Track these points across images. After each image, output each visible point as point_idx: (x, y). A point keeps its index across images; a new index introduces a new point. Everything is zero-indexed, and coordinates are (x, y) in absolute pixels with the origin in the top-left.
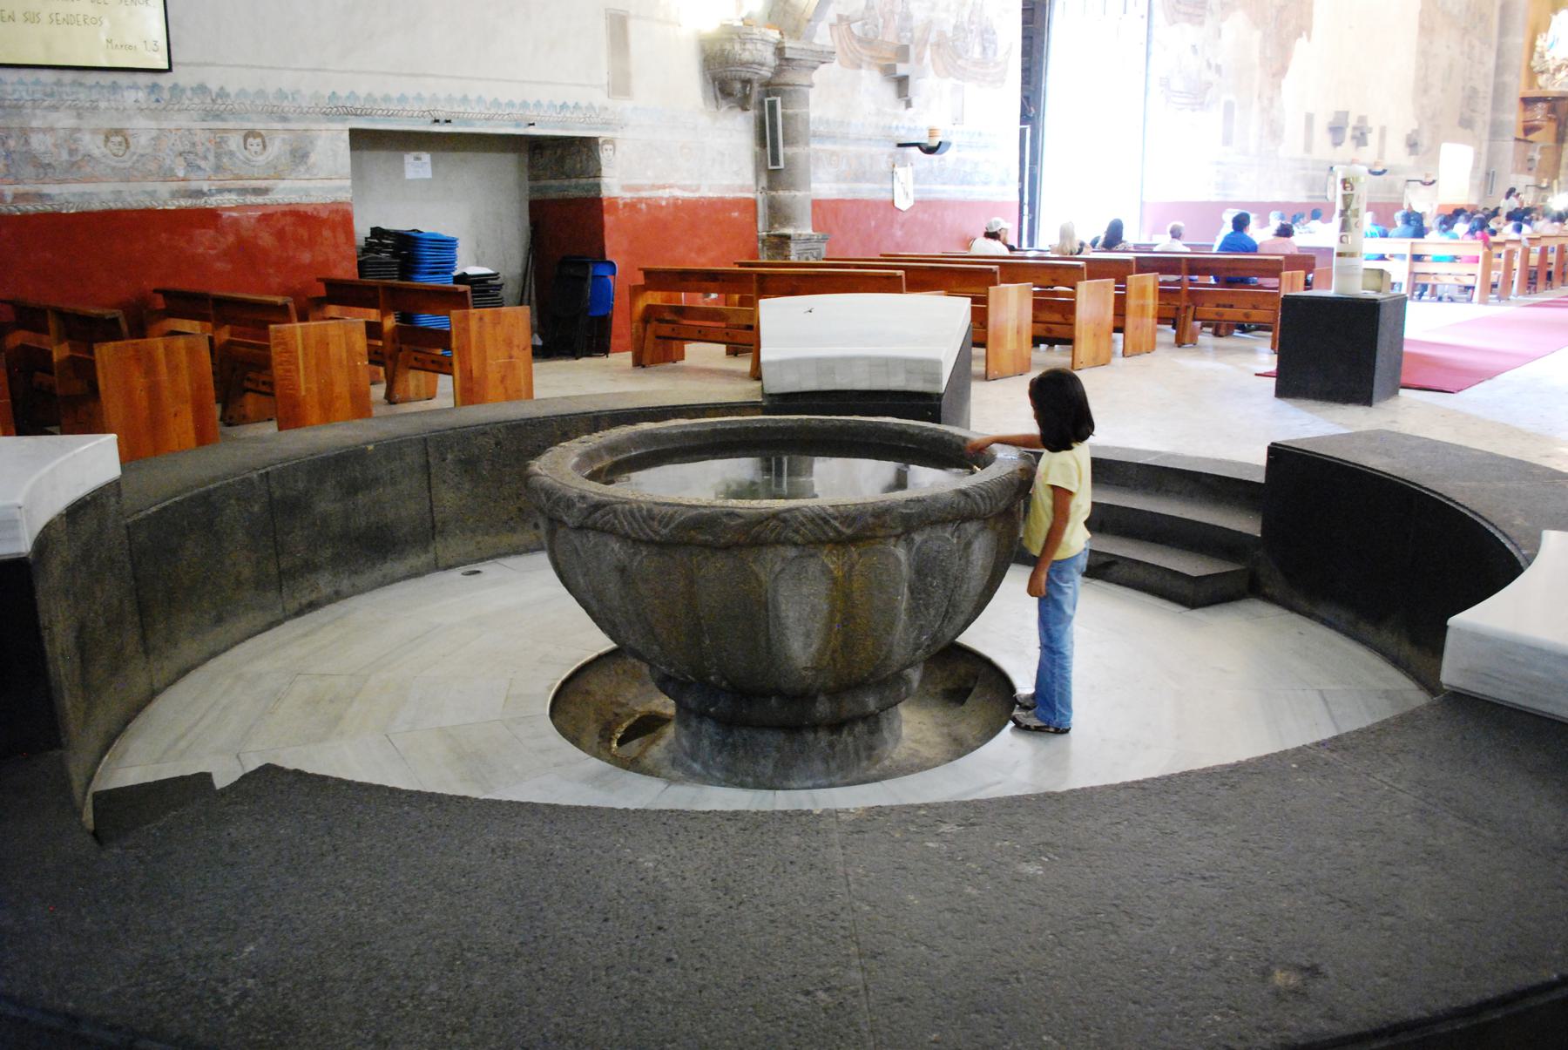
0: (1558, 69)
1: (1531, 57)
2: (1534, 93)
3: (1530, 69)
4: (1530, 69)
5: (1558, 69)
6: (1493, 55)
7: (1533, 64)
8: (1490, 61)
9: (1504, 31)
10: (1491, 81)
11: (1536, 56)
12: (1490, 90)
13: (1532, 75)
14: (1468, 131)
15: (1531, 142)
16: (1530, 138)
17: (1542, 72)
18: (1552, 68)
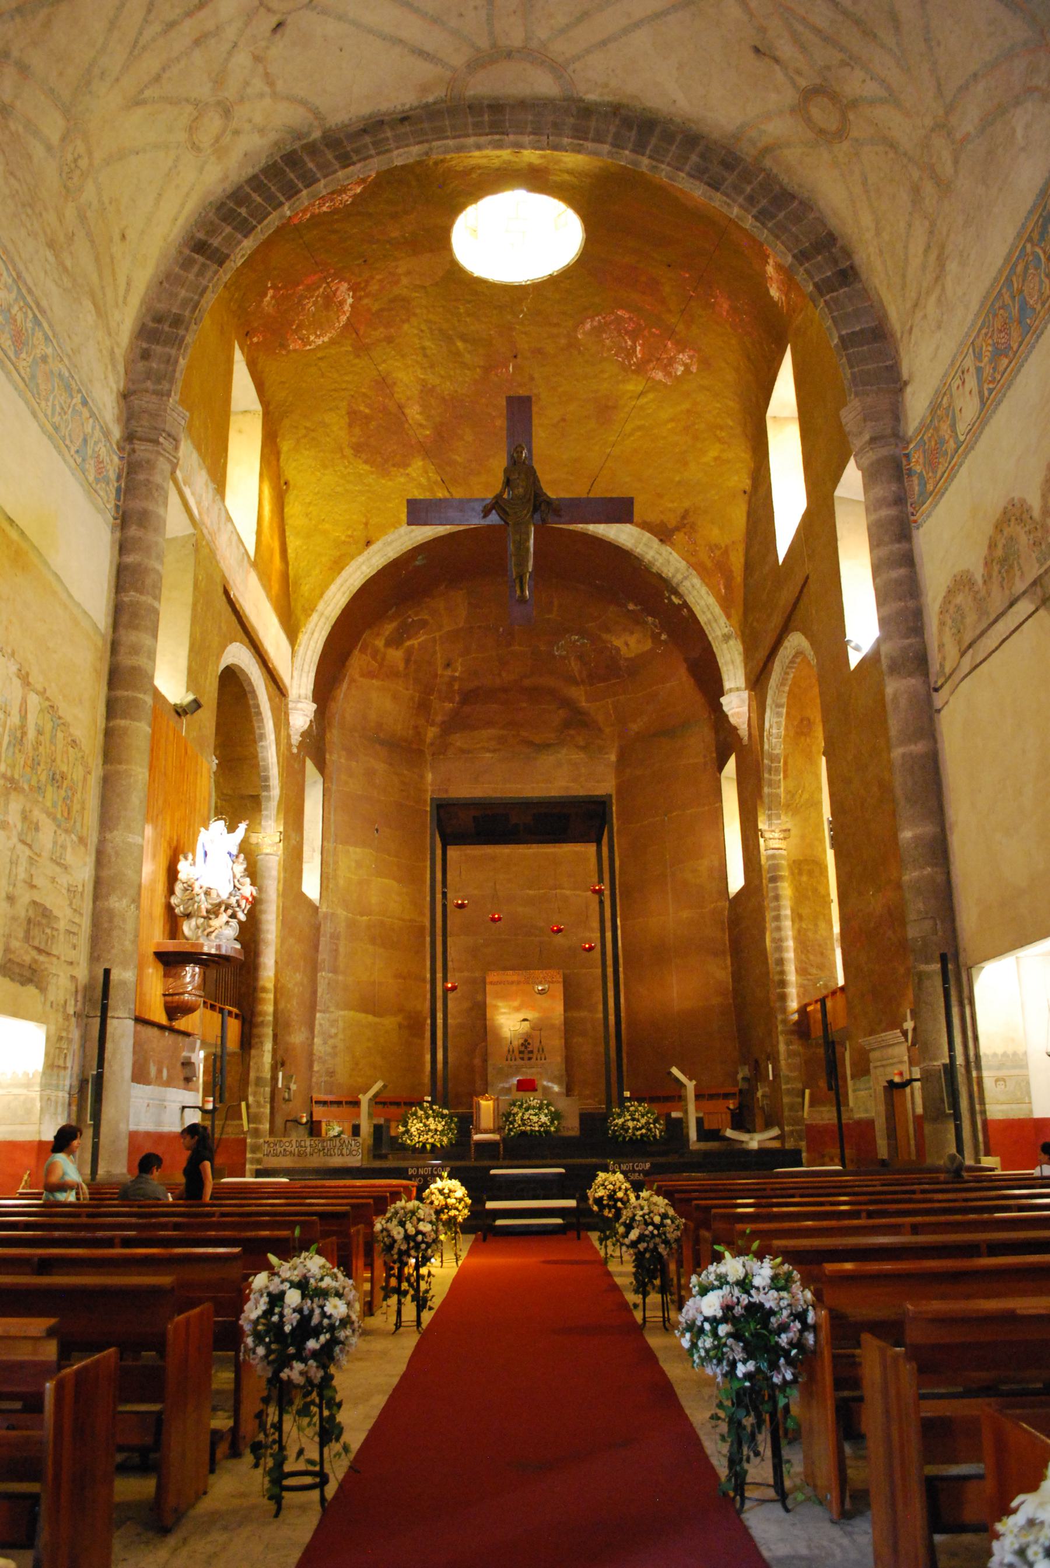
0: (214, 911)
1: (171, 892)
2: (171, 946)
3: (169, 908)
4: (169, 908)
5: (214, 911)
6: (90, 859)
7: (174, 901)
8: (83, 872)
9: (106, 820)
10: (87, 906)
11: (178, 887)
12: (86, 923)
13: (173, 921)
14: (31, 989)
15: (187, 1034)
16: (182, 1024)
17: (188, 916)
18: (205, 906)
